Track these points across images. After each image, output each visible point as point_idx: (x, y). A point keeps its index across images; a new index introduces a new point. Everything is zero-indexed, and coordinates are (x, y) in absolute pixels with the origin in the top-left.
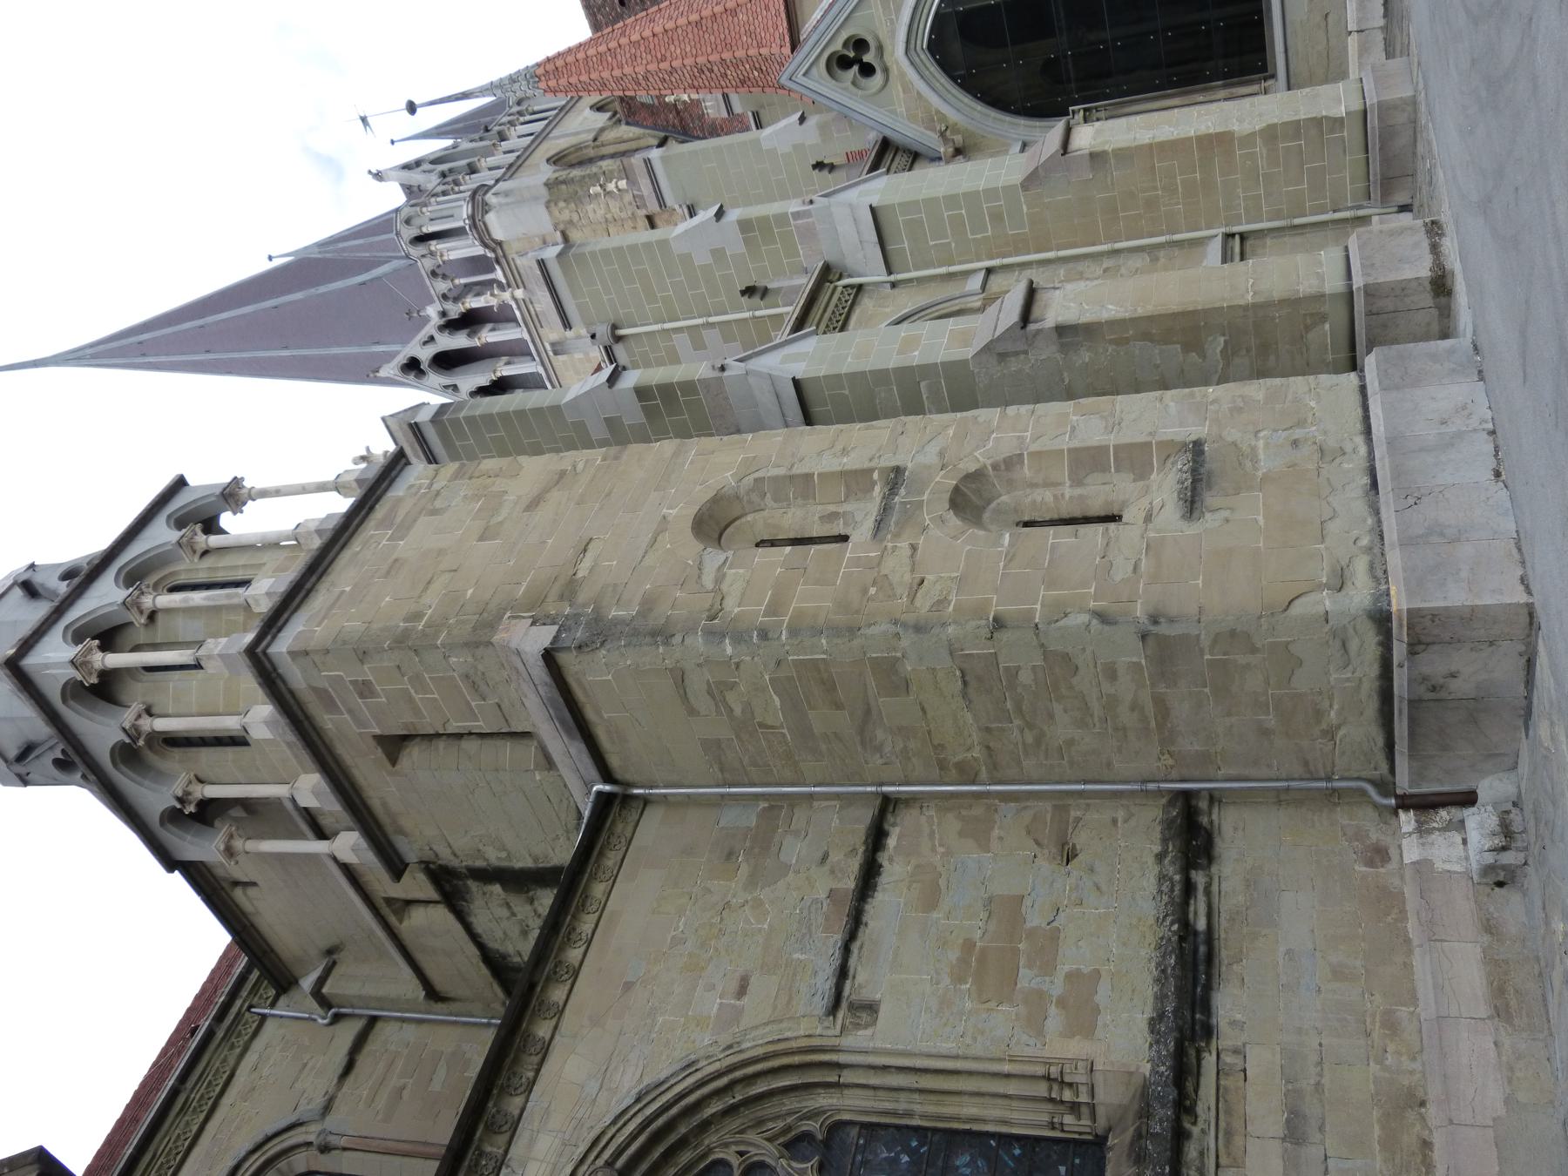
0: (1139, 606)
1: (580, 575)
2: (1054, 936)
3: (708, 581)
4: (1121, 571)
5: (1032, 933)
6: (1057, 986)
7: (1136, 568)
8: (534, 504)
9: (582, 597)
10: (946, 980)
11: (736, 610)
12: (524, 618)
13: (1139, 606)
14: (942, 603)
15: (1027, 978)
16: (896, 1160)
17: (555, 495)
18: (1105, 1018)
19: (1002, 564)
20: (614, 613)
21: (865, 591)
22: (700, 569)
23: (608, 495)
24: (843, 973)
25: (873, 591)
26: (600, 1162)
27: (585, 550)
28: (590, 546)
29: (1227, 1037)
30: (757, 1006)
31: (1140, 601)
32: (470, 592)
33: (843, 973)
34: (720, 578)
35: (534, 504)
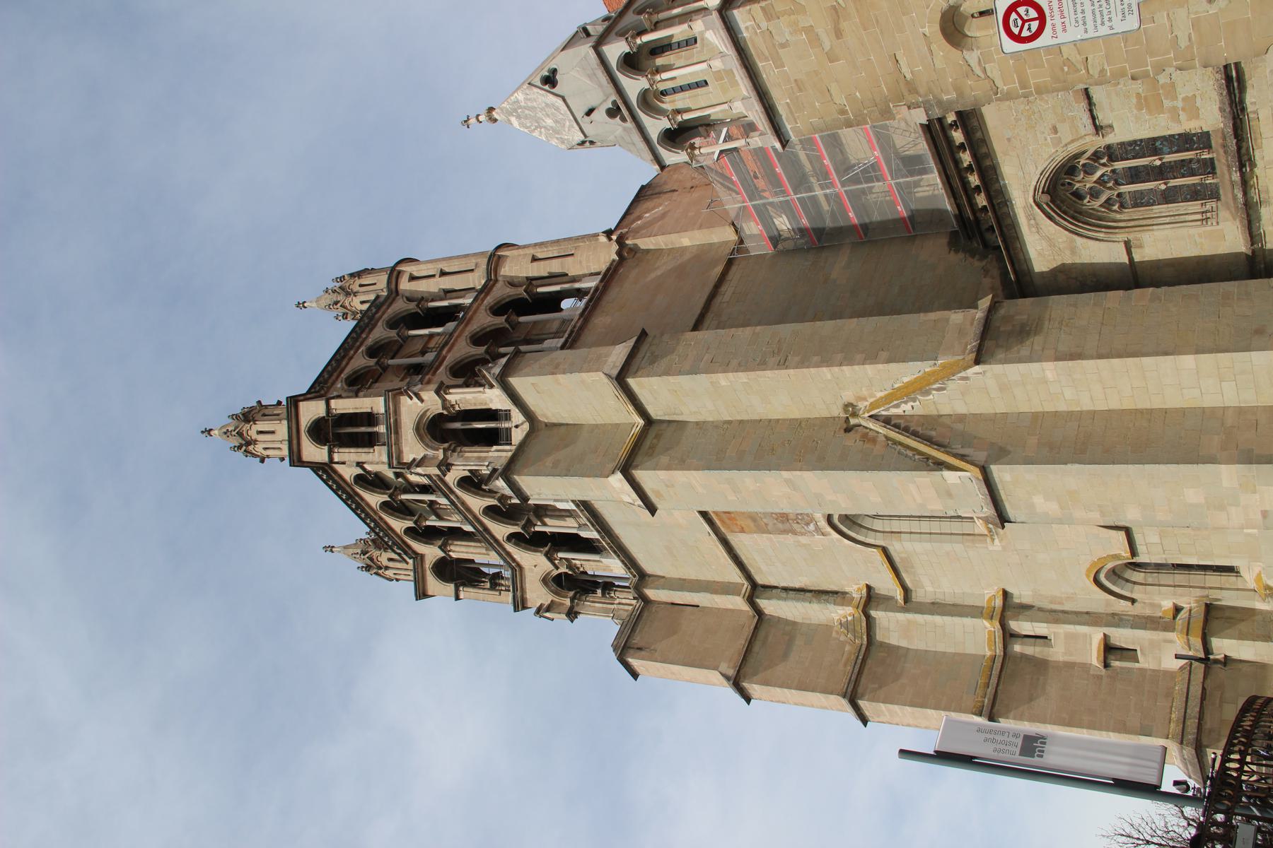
0: (1197, 62)
1: (909, 76)
2: (1173, 85)
3: (978, 71)
4: (1183, 43)
5: (1162, 87)
6: (1180, 104)
7: (1190, 39)
8: (838, 34)
9: (922, 90)
10: (1135, 111)
11: (1005, 88)
12: (901, 105)
13: (1197, 62)
14: (1102, 71)
15: (1167, 103)
16: (1134, 148)
17: (844, 25)
18: (1202, 111)
19: (1122, 44)
20: (945, 98)
21: (1063, 70)
22: (969, 65)
23: (877, 21)
24: (1093, 118)
25: (1066, 69)
26: (1040, 193)
27: (897, 61)
28: (897, 58)
29: (1250, 108)
30: (1066, 134)
31: (1197, 59)
32: (857, 94)
33: (1093, 118)
34: (985, 71)
35: (838, 34)
